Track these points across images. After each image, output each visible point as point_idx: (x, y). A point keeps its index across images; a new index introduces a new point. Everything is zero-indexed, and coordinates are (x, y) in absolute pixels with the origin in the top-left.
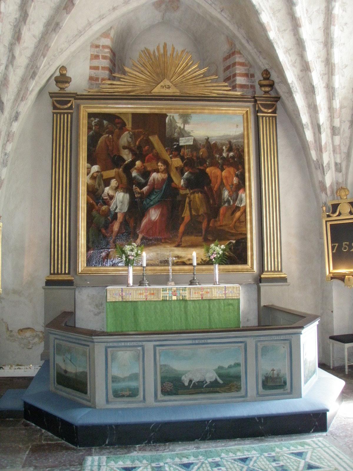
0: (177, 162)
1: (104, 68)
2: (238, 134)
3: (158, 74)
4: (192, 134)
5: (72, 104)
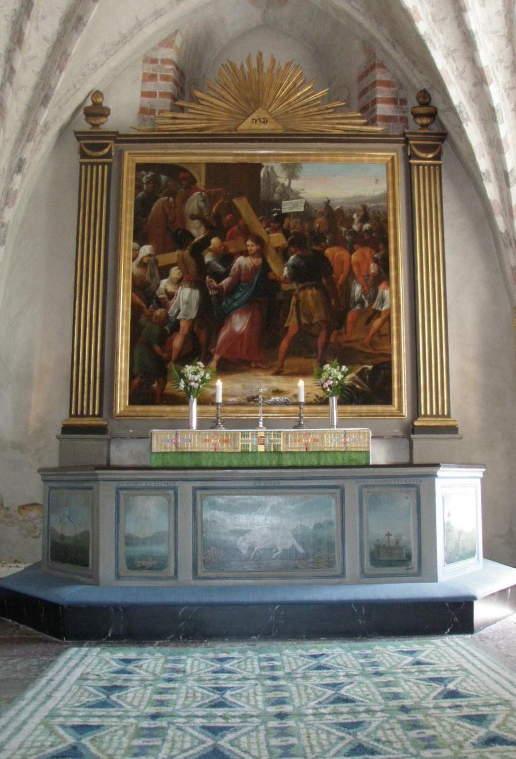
0: (277, 239)
1: (163, 95)
2: (377, 193)
3: (247, 101)
4: (302, 195)
5: (110, 150)
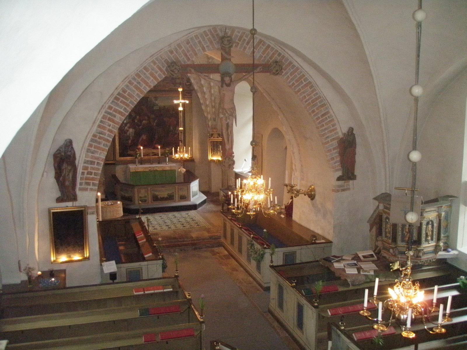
0: (153, 116)
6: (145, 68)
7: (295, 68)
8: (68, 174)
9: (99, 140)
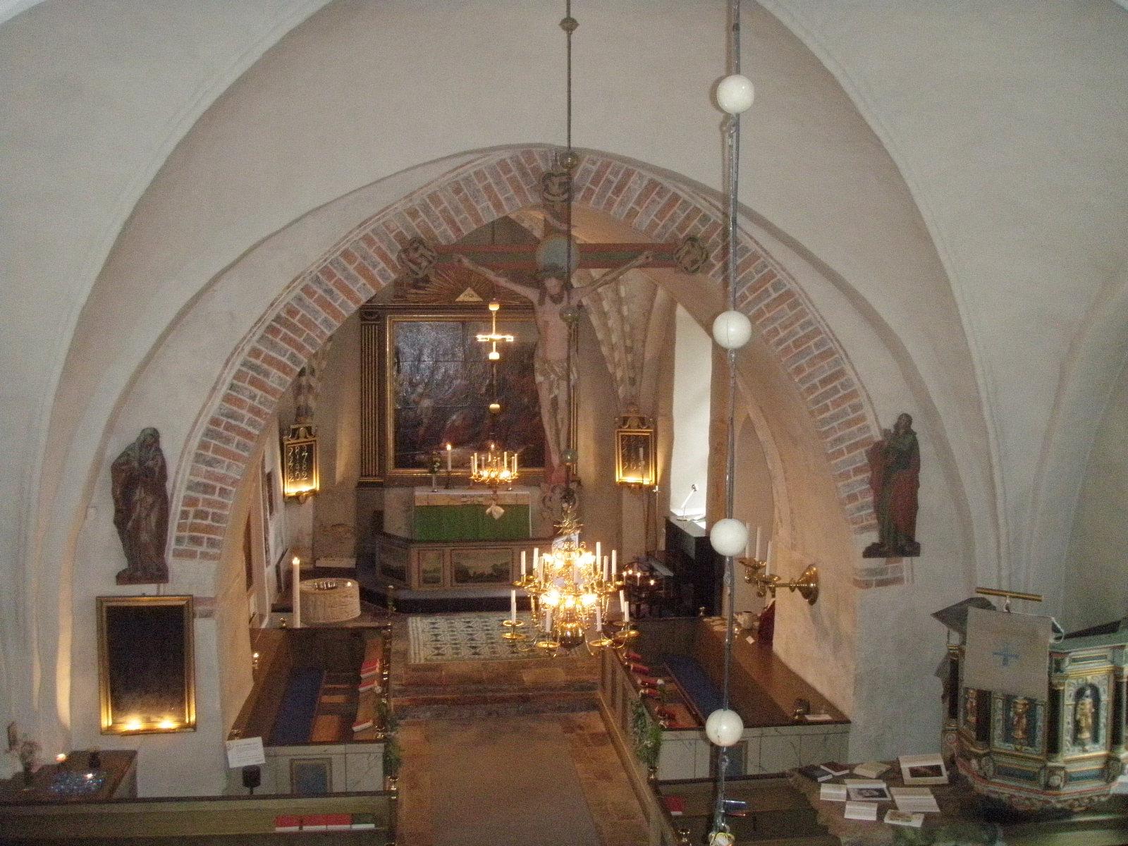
6: (346, 254)
7: (749, 253)
8: (148, 515)
9: (225, 433)
